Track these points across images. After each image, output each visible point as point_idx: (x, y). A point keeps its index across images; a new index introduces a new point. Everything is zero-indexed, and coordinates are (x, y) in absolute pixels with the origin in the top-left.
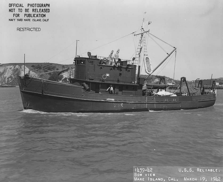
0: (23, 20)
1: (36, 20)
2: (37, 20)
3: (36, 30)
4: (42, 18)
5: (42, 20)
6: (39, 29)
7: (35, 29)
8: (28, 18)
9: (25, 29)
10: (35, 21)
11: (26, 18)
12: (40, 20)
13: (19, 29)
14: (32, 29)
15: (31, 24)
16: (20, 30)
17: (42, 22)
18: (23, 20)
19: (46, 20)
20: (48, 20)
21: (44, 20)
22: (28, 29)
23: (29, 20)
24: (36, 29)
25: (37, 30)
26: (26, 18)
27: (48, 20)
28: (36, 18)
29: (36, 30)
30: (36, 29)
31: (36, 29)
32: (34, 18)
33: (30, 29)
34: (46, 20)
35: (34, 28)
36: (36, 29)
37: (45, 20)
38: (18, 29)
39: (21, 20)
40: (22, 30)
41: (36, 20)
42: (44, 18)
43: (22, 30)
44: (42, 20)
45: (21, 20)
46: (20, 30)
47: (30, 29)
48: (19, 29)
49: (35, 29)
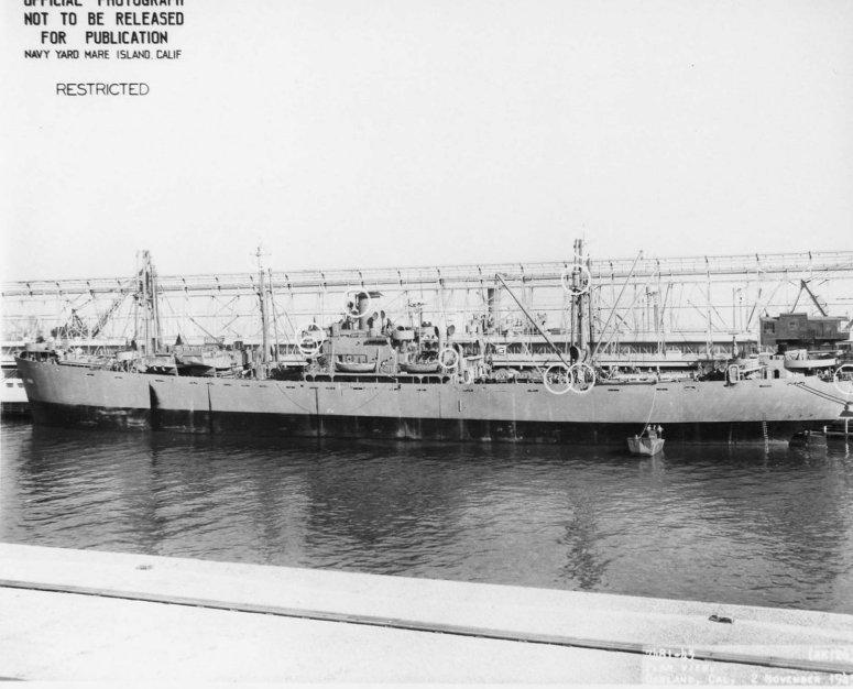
3: (133, 92)
6: (144, 89)
7: (127, 87)
9: (87, 87)
10: (126, 56)
13: (66, 89)
14: (114, 89)
15: (112, 69)
16: (71, 92)
17: (153, 62)
19: (172, 55)
22: (101, 87)
24: (132, 86)
25: (136, 89)
29: (133, 92)
30: (130, 88)
31: (132, 86)
33: (107, 89)
34: (172, 55)
36: (130, 88)
38: (60, 87)
40: (75, 90)
46: (71, 92)
47: (107, 89)
48: (66, 89)
49: (127, 87)
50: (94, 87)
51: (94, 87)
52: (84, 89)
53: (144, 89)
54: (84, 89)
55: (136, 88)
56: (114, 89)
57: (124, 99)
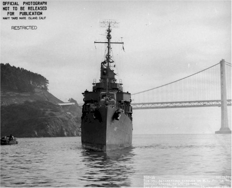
0: (19, 18)
1: (32, 18)
2: (33, 18)
4: (38, 16)
5: (38, 18)
6: (36, 28)
7: (31, 27)
8: (24, 16)
9: (20, 27)
10: (31, 19)
11: (22, 16)
12: (36, 18)
14: (27, 28)
15: (27, 22)
17: (38, 20)
18: (19, 18)
19: (43, 18)
20: (45, 18)
21: (40, 18)
22: (24, 27)
23: (25, 18)
26: (22, 16)
27: (45, 18)
28: (32, 16)
30: (32, 27)
32: (30, 16)
33: (25, 28)
35: (30, 26)
36: (32, 27)
37: (41, 18)
39: (16, 18)
40: (17, 28)
41: (32, 18)
42: (41, 16)
43: (17, 28)
44: (38, 18)
45: (16, 18)
47: (25, 28)
50: (22, 27)
51: (22, 27)
52: (19, 28)
53: (36, 28)
54: (19, 28)
55: (34, 28)
56: (27, 28)
57: (30, 30)
